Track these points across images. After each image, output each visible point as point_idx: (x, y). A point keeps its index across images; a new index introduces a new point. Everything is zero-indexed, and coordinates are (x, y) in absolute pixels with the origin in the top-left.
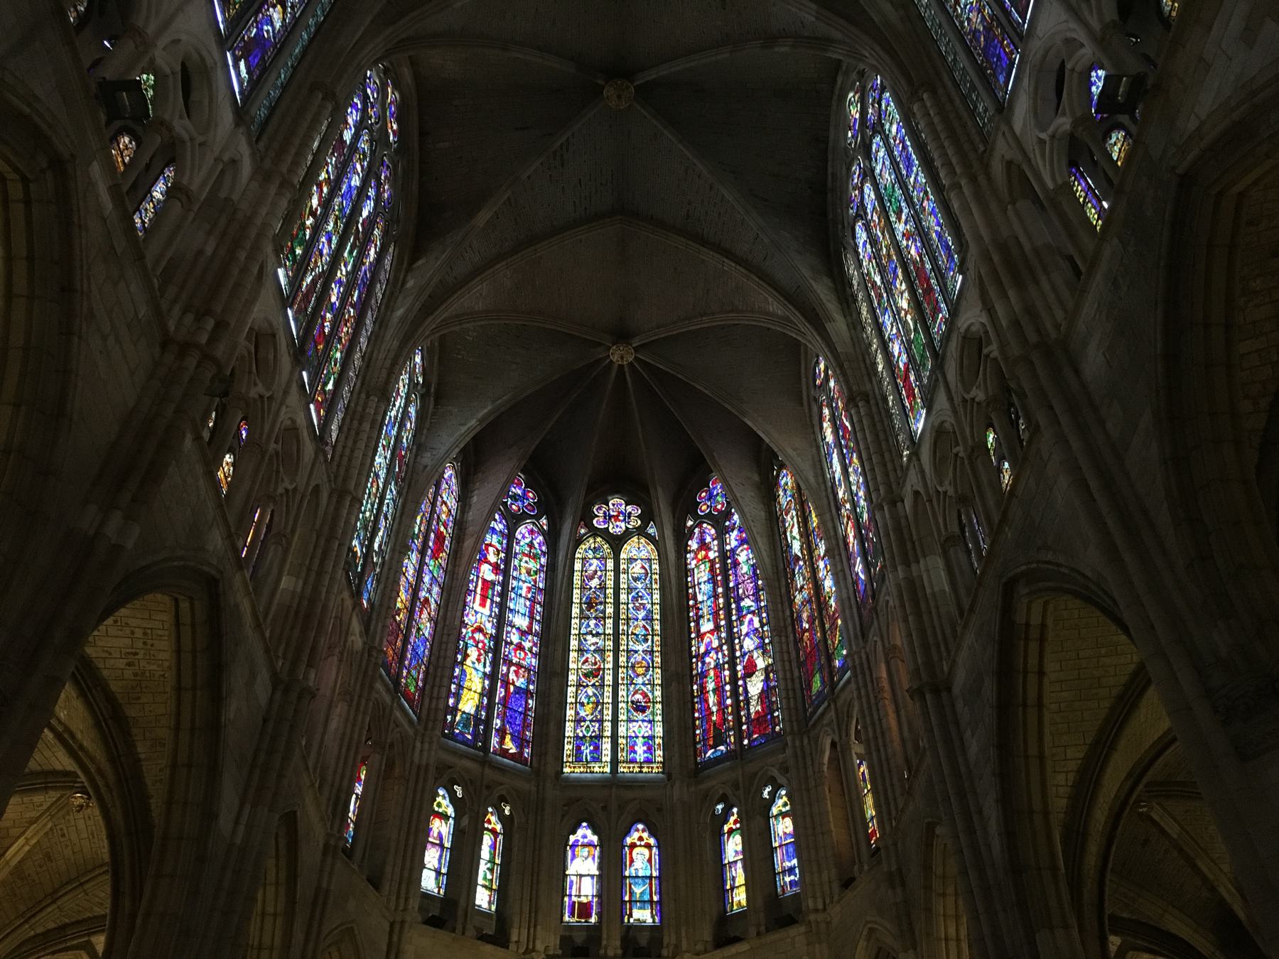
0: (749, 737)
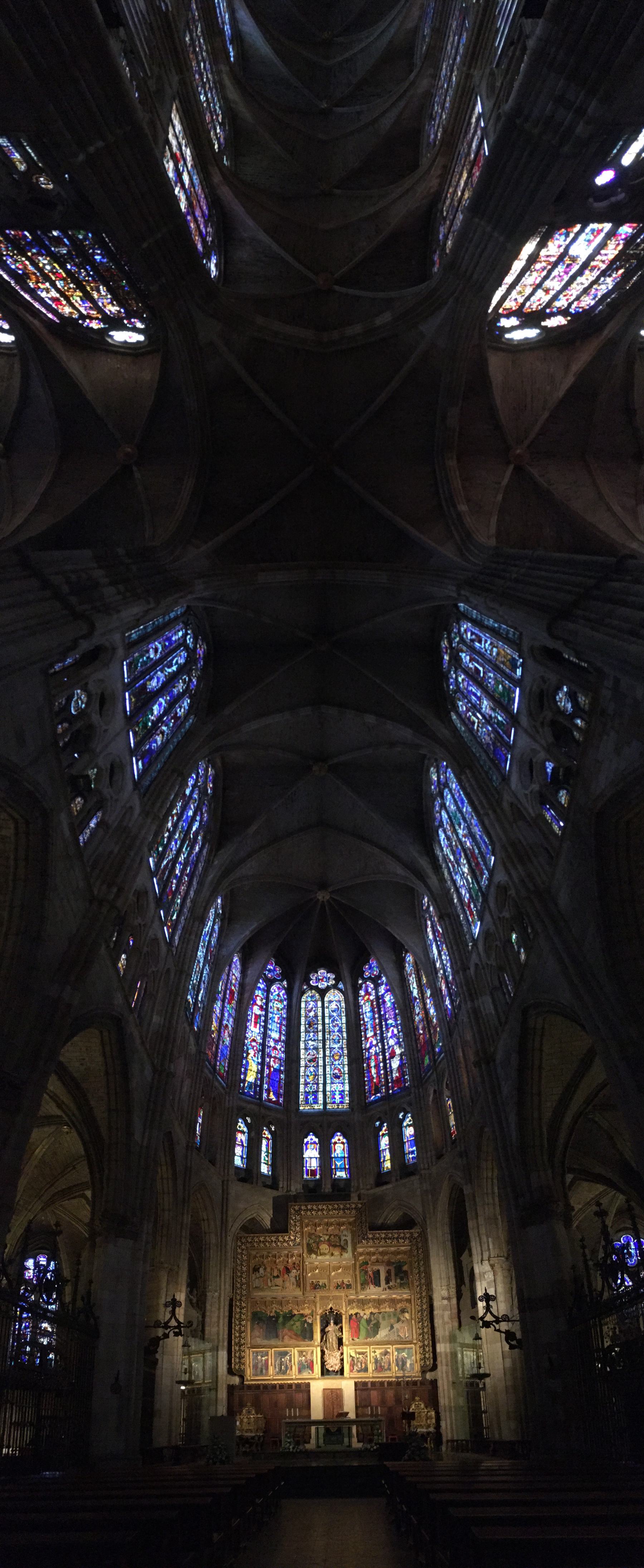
0: (393, 1088)
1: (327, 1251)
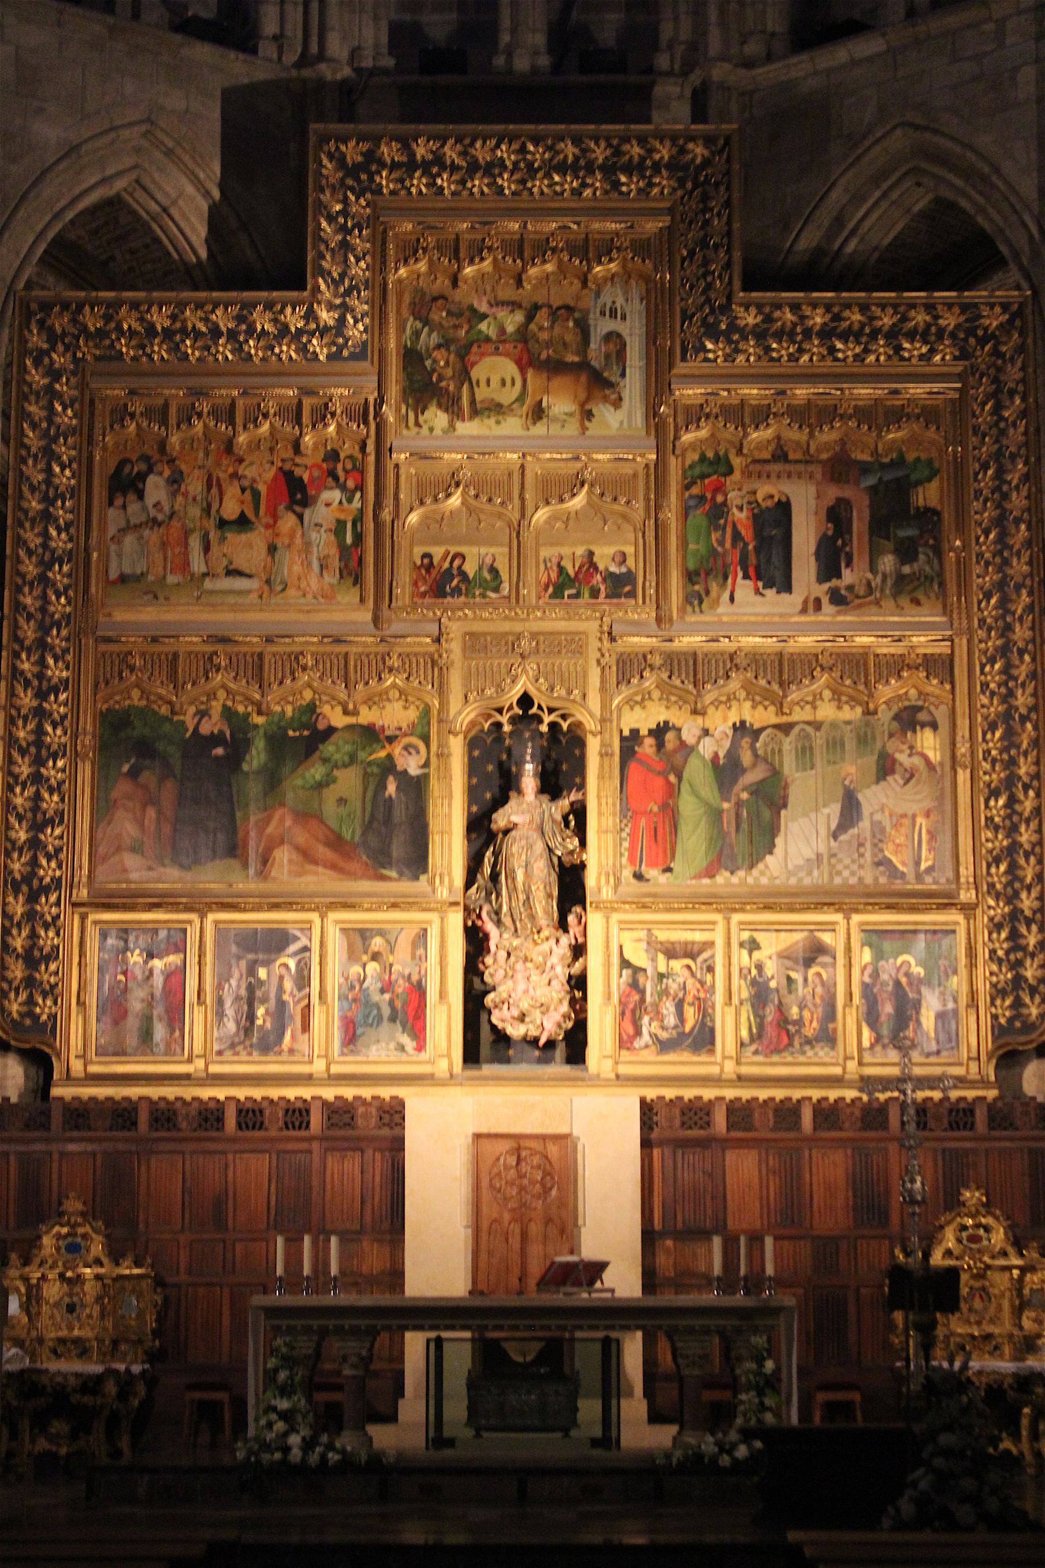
1: (508, 396)
